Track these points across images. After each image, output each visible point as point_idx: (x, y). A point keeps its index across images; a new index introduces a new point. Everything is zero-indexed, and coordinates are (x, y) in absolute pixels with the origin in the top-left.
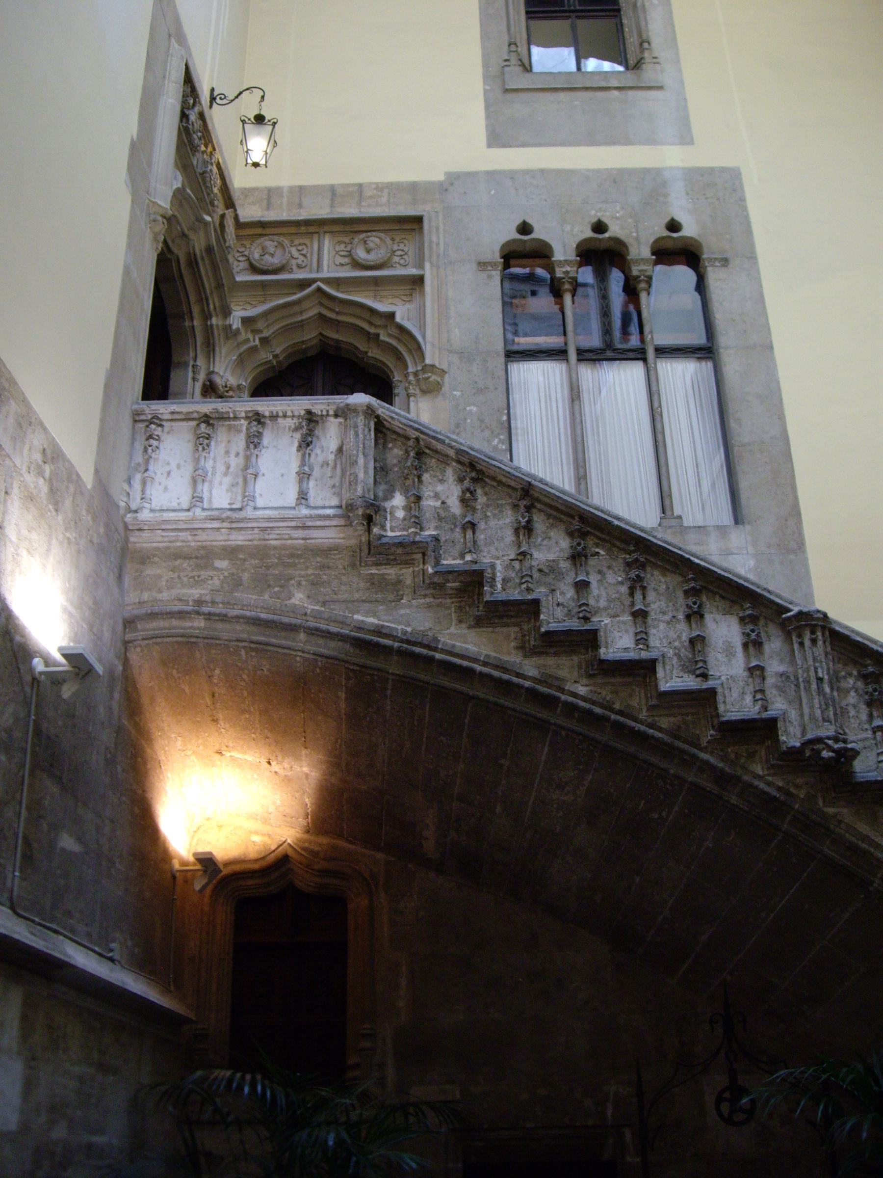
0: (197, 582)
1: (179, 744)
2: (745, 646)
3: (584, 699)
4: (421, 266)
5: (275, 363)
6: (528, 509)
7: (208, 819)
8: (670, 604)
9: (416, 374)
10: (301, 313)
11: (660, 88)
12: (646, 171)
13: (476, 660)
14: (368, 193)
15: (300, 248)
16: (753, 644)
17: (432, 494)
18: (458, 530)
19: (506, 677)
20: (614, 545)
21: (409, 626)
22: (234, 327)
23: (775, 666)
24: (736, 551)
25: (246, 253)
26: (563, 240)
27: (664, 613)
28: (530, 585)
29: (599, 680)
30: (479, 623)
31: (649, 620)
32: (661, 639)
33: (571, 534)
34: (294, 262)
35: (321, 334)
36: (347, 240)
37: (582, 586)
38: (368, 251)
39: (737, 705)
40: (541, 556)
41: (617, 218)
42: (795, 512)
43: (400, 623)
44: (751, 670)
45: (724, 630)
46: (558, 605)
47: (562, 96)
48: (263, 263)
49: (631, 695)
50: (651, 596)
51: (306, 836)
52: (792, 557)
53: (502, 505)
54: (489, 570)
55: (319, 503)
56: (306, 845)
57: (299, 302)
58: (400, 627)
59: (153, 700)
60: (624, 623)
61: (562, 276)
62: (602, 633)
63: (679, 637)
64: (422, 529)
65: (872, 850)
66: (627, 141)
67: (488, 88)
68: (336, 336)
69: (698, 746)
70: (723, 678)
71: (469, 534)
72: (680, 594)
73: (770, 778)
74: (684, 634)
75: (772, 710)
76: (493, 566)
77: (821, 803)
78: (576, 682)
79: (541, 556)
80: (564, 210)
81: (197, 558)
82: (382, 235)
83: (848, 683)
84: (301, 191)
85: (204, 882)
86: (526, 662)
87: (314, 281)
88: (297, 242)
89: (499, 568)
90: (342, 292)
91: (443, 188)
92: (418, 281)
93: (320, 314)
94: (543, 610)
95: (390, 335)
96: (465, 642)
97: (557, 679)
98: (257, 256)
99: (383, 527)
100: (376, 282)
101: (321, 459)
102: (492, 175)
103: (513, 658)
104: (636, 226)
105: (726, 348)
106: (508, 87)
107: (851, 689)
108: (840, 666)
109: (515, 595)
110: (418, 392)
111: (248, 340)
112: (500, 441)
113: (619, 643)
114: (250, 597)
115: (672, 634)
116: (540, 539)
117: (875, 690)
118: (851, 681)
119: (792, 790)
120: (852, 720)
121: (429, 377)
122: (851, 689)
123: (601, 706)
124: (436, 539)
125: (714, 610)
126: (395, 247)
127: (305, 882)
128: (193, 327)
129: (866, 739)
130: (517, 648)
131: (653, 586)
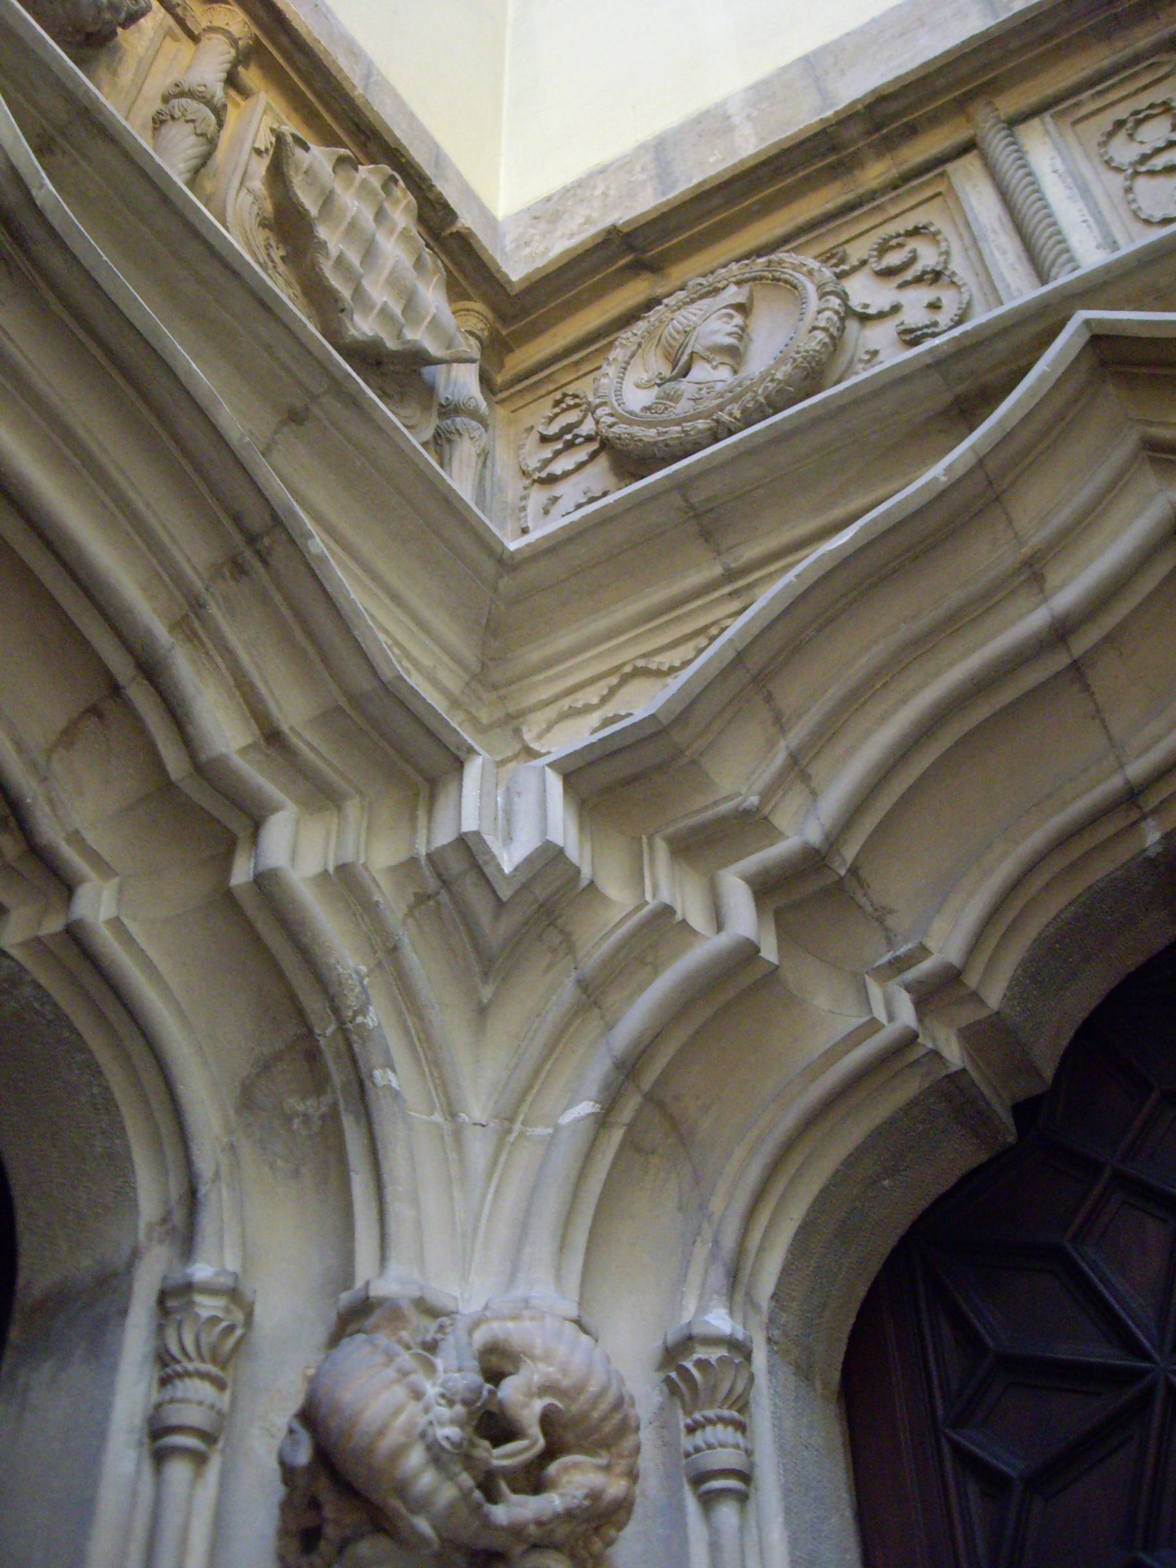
5: (954, 1054)
10: (1032, 573)
15: (894, 259)
22: (509, 858)
25: (588, 427)
34: (880, 336)
48: (683, 407)
88: (857, 251)
111: (662, 925)
128: (76, 936)
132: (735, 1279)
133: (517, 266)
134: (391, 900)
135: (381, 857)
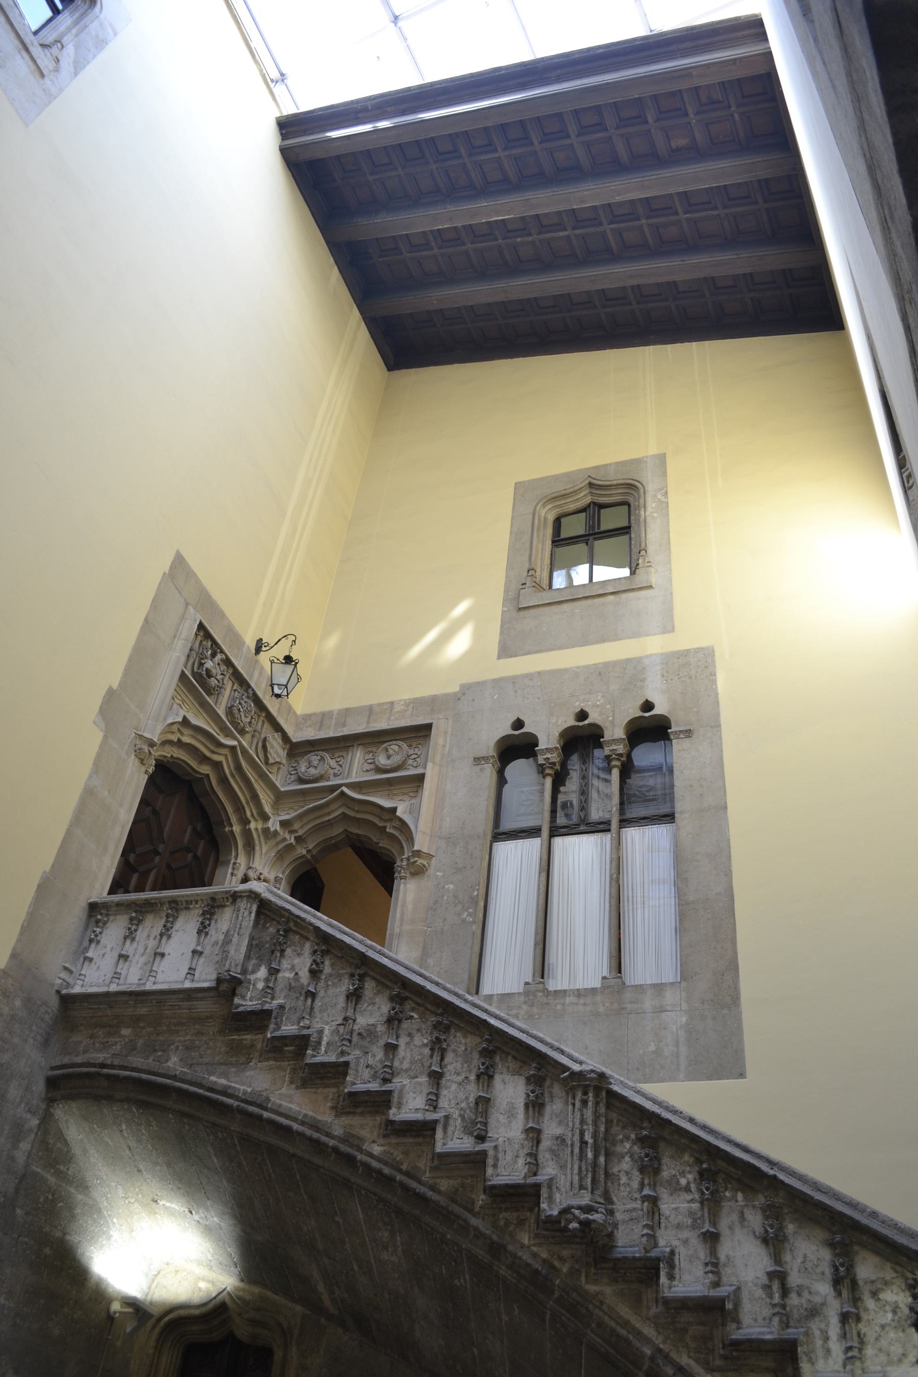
0: (105, 1046)
1: (120, 1192)
2: (527, 1106)
3: (379, 1160)
4: (425, 768)
5: (309, 857)
6: (362, 977)
7: (167, 1264)
8: (466, 1065)
9: (408, 859)
10: (329, 814)
11: (650, 587)
12: (628, 661)
13: (295, 1120)
14: (397, 708)
16: (535, 1106)
17: (289, 967)
18: (302, 998)
19: (316, 1135)
20: (427, 1009)
21: (250, 1086)
22: (272, 829)
23: (551, 1129)
24: (669, 1008)
26: (548, 733)
27: (458, 1074)
28: (344, 1048)
29: (394, 1140)
30: (304, 1084)
31: (443, 1082)
32: (450, 1100)
33: (392, 999)
35: (346, 830)
36: (374, 749)
37: (391, 1049)
38: (389, 757)
39: (509, 1170)
40: (362, 1021)
41: (598, 706)
42: (733, 966)
43: (243, 1084)
44: (528, 1131)
45: (510, 1090)
46: (367, 1067)
47: (565, 607)
49: (419, 1157)
50: (450, 1057)
51: (242, 1285)
52: (725, 1011)
53: (342, 974)
54: (315, 1035)
55: (204, 977)
56: (241, 1293)
57: (327, 804)
58: (242, 1088)
59: (85, 1151)
60: (420, 1084)
61: (544, 762)
62: (396, 1095)
63: (467, 1098)
64: (273, 998)
65: (631, 1337)
66: (616, 638)
67: (505, 609)
68: (356, 831)
69: (471, 1211)
70: (501, 1140)
71: (309, 1001)
72: (476, 1055)
73: (535, 1249)
74: (472, 1095)
75: (543, 1175)
76: (321, 1032)
77: (583, 1279)
78: (374, 1142)
79: (362, 1021)
80: (552, 705)
81: (110, 1026)
82: (401, 743)
83: (624, 1147)
84: (347, 712)
85: (135, 1324)
86: (336, 1122)
87: (341, 785)
89: (326, 1032)
90: (363, 794)
91: (457, 698)
92: (420, 778)
93: (343, 813)
94: (351, 1072)
95: (394, 827)
96: (290, 1102)
97: (358, 1138)
98: (303, 769)
99: (243, 997)
100: (389, 782)
101: (213, 939)
102: (497, 682)
103: (325, 1116)
104: (613, 711)
105: (681, 813)
106: (520, 606)
107: (627, 1153)
108: (619, 1128)
109: (332, 1058)
110: (408, 875)
112: (470, 915)
113: (411, 1105)
114: (137, 1061)
115: (462, 1096)
116: (366, 1005)
117: (647, 1155)
118: (628, 1145)
119: (556, 1263)
120: (622, 1188)
121: (416, 861)
122: (627, 1153)
123: (392, 1167)
124: (282, 1007)
125: (505, 1070)
126: (411, 752)
127: (243, 1332)
129: (634, 1209)
130: (332, 1108)
131: (453, 1047)
132: (283, 873)
133: (296, 736)
134: (260, 831)
135: (260, 826)
